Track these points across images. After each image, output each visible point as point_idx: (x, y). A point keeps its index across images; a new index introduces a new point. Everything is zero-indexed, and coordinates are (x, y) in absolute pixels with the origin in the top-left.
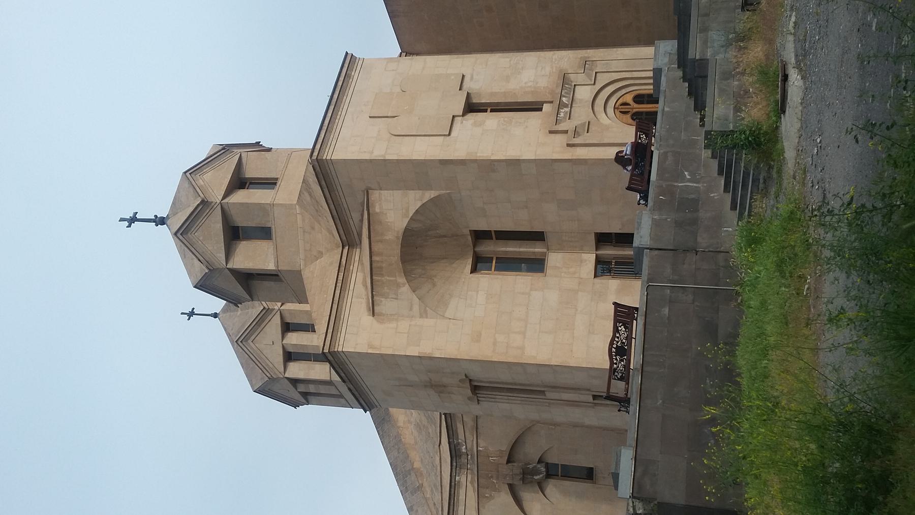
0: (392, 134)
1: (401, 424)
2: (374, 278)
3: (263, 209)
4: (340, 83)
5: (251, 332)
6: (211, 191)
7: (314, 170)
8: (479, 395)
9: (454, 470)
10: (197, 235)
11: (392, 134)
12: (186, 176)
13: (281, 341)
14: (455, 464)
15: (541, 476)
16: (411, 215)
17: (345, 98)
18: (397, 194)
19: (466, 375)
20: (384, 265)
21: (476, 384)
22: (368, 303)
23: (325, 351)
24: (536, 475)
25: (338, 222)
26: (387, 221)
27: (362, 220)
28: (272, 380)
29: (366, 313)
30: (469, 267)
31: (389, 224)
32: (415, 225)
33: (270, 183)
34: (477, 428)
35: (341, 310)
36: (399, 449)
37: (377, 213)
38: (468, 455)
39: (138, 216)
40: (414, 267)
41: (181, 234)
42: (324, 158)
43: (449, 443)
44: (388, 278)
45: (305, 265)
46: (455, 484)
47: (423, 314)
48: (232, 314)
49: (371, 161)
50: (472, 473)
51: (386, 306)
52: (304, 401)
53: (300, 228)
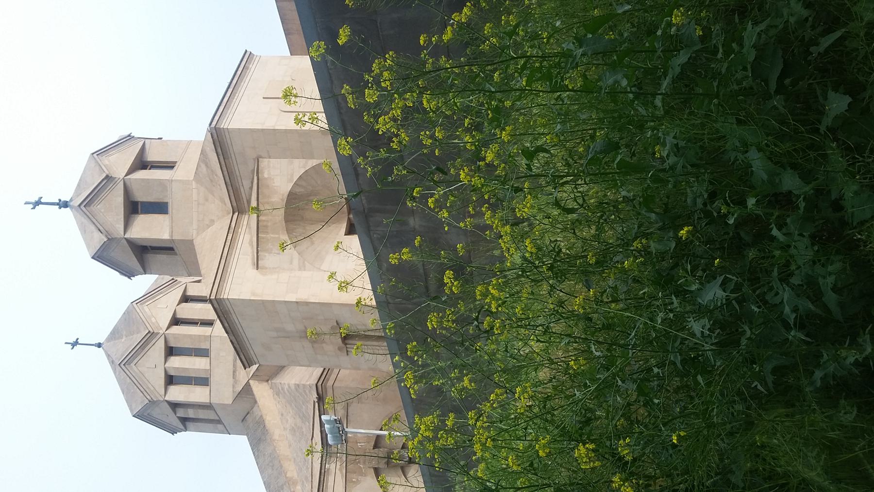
0: (281, 111)
1: (276, 437)
2: (260, 235)
3: (162, 183)
4: (239, 72)
5: (135, 355)
6: (115, 169)
7: (212, 137)
8: (347, 346)
10: (98, 208)
11: (281, 111)
12: (81, 209)
13: (163, 364)
16: (295, 181)
17: (242, 83)
18: (284, 162)
19: (337, 321)
20: (269, 224)
23: (211, 298)
25: (230, 188)
26: (274, 185)
27: (251, 188)
28: (152, 403)
30: (343, 230)
31: (275, 188)
32: (298, 190)
33: (169, 166)
34: (347, 416)
35: (229, 263)
36: (273, 466)
39: (42, 200)
40: (295, 227)
41: (84, 206)
42: (222, 127)
44: (272, 235)
45: (198, 234)
46: (325, 471)
47: (302, 267)
48: (116, 341)
49: (263, 130)
51: (269, 260)
52: (183, 428)
53: (195, 201)
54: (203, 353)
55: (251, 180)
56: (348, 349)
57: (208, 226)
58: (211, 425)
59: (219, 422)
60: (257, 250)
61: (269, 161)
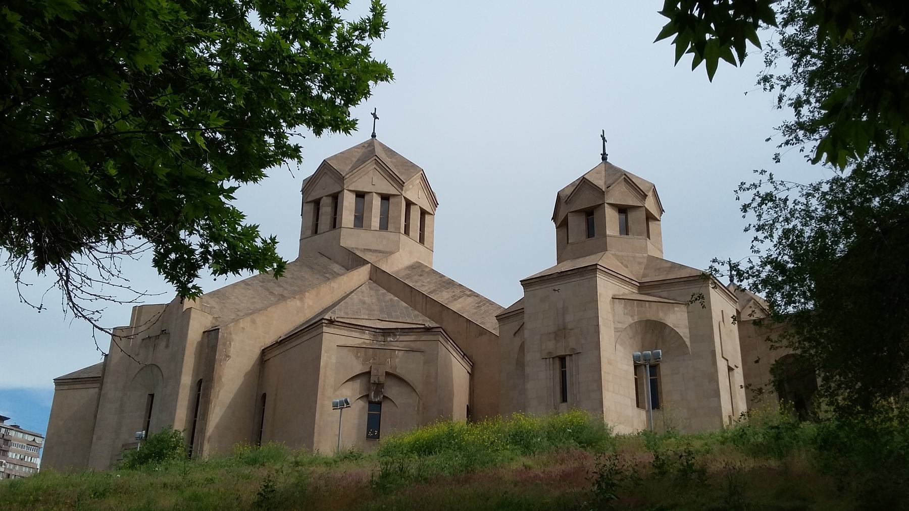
2: (636, 302)
5: (384, 169)
8: (551, 359)
9: (373, 330)
14: (378, 331)
15: (373, 398)
21: (568, 359)
22: (618, 296)
24: (374, 393)
28: (341, 179)
29: (613, 293)
34: (413, 351)
37: (674, 309)
38: (384, 342)
43: (397, 329)
45: (613, 255)
47: (617, 330)
50: (370, 344)
51: (619, 306)
52: (309, 200)
54: (384, 226)
55: (667, 297)
56: (548, 359)
57: (622, 263)
58: (310, 223)
59: (316, 231)
60: (626, 299)
61: (685, 312)
